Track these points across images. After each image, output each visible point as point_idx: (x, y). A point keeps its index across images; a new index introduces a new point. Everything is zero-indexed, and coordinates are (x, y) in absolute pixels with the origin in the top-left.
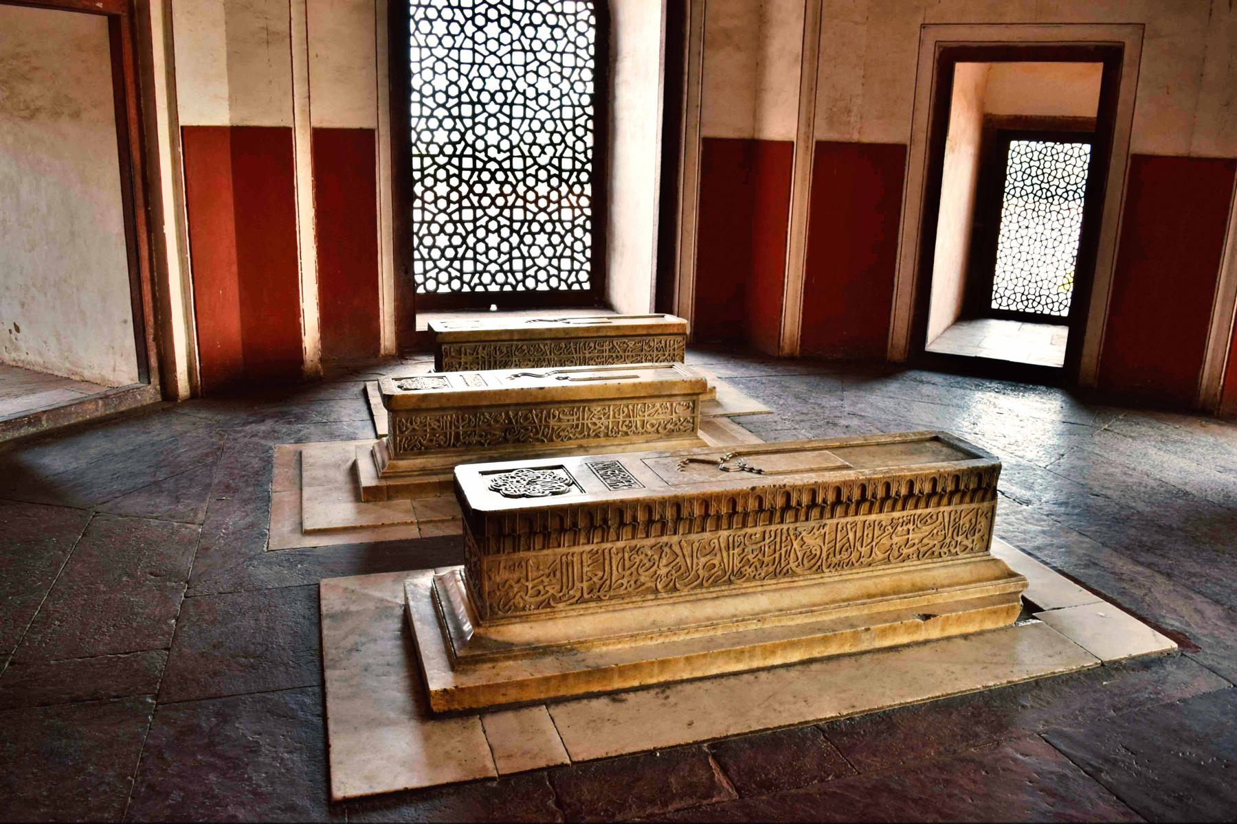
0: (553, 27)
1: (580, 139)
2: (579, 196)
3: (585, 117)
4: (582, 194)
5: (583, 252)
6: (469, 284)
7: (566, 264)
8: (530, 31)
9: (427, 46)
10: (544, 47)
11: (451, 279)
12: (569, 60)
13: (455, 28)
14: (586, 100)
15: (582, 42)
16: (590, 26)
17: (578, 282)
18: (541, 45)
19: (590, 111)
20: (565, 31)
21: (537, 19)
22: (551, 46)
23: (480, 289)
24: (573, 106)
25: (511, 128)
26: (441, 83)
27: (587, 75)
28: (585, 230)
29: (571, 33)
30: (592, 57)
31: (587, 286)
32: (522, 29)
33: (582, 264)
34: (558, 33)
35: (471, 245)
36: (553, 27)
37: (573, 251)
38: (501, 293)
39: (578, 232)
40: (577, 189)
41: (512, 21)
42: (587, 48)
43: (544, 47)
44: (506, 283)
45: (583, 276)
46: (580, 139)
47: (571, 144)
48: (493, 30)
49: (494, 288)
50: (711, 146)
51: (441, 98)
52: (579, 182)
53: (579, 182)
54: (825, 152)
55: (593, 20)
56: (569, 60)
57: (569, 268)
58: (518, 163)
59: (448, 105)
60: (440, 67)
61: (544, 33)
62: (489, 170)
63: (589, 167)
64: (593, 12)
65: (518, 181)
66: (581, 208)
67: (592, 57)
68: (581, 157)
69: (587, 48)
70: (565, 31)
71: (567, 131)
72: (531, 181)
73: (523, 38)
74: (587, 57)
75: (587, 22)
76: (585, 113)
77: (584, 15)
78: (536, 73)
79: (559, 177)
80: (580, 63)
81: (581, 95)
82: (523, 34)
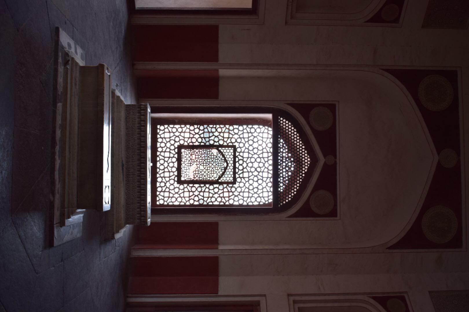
0: (257, 188)
4: (194, 201)
6: (160, 155)
7: (167, 194)
8: (256, 179)
9: (249, 140)
11: (162, 148)
12: (246, 195)
15: (253, 199)
18: (251, 183)
21: (260, 182)
23: (158, 159)
27: (241, 202)
28: (180, 202)
30: (248, 204)
31: (158, 203)
34: (256, 190)
37: (172, 197)
39: (179, 199)
40: (196, 199)
41: (259, 172)
42: (251, 202)
44: (160, 169)
45: (161, 202)
47: (214, 196)
48: (256, 165)
50: (215, 225)
54: (215, 260)
55: (261, 203)
56: (246, 195)
57: (165, 196)
61: (255, 185)
64: (264, 204)
67: (248, 204)
68: (209, 200)
69: (251, 202)
71: (219, 194)
74: (248, 202)
76: (226, 201)
77: (263, 201)
79: (201, 191)
80: (245, 199)
82: (255, 176)
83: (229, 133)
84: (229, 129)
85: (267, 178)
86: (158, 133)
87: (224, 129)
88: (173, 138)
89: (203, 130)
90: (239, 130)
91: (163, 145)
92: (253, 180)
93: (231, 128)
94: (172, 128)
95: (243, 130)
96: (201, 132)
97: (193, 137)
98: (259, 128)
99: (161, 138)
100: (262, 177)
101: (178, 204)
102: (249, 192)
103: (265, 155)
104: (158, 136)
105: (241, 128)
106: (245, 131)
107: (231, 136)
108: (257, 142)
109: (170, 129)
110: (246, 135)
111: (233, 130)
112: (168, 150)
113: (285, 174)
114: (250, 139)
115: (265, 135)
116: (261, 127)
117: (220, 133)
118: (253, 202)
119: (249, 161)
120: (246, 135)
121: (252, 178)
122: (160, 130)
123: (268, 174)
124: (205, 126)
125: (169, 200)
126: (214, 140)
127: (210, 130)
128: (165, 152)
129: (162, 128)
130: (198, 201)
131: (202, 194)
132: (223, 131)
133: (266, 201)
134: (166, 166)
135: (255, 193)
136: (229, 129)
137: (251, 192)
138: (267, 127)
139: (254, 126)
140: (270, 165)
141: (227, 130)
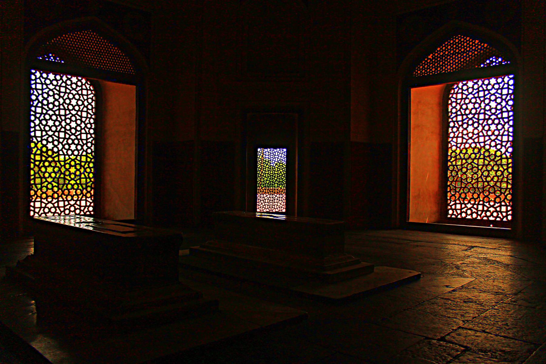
26: (470, 129)
38: (495, 221)
44: (497, 217)
49: (491, 218)
60: (470, 122)
84: (453, 138)
87: (453, 144)
93: (452, 135)
98: (451, 104)
110: (460, 118)
120: (460, 118)
128: (477, 209)
136: (453, 138)
141: (455, 140)
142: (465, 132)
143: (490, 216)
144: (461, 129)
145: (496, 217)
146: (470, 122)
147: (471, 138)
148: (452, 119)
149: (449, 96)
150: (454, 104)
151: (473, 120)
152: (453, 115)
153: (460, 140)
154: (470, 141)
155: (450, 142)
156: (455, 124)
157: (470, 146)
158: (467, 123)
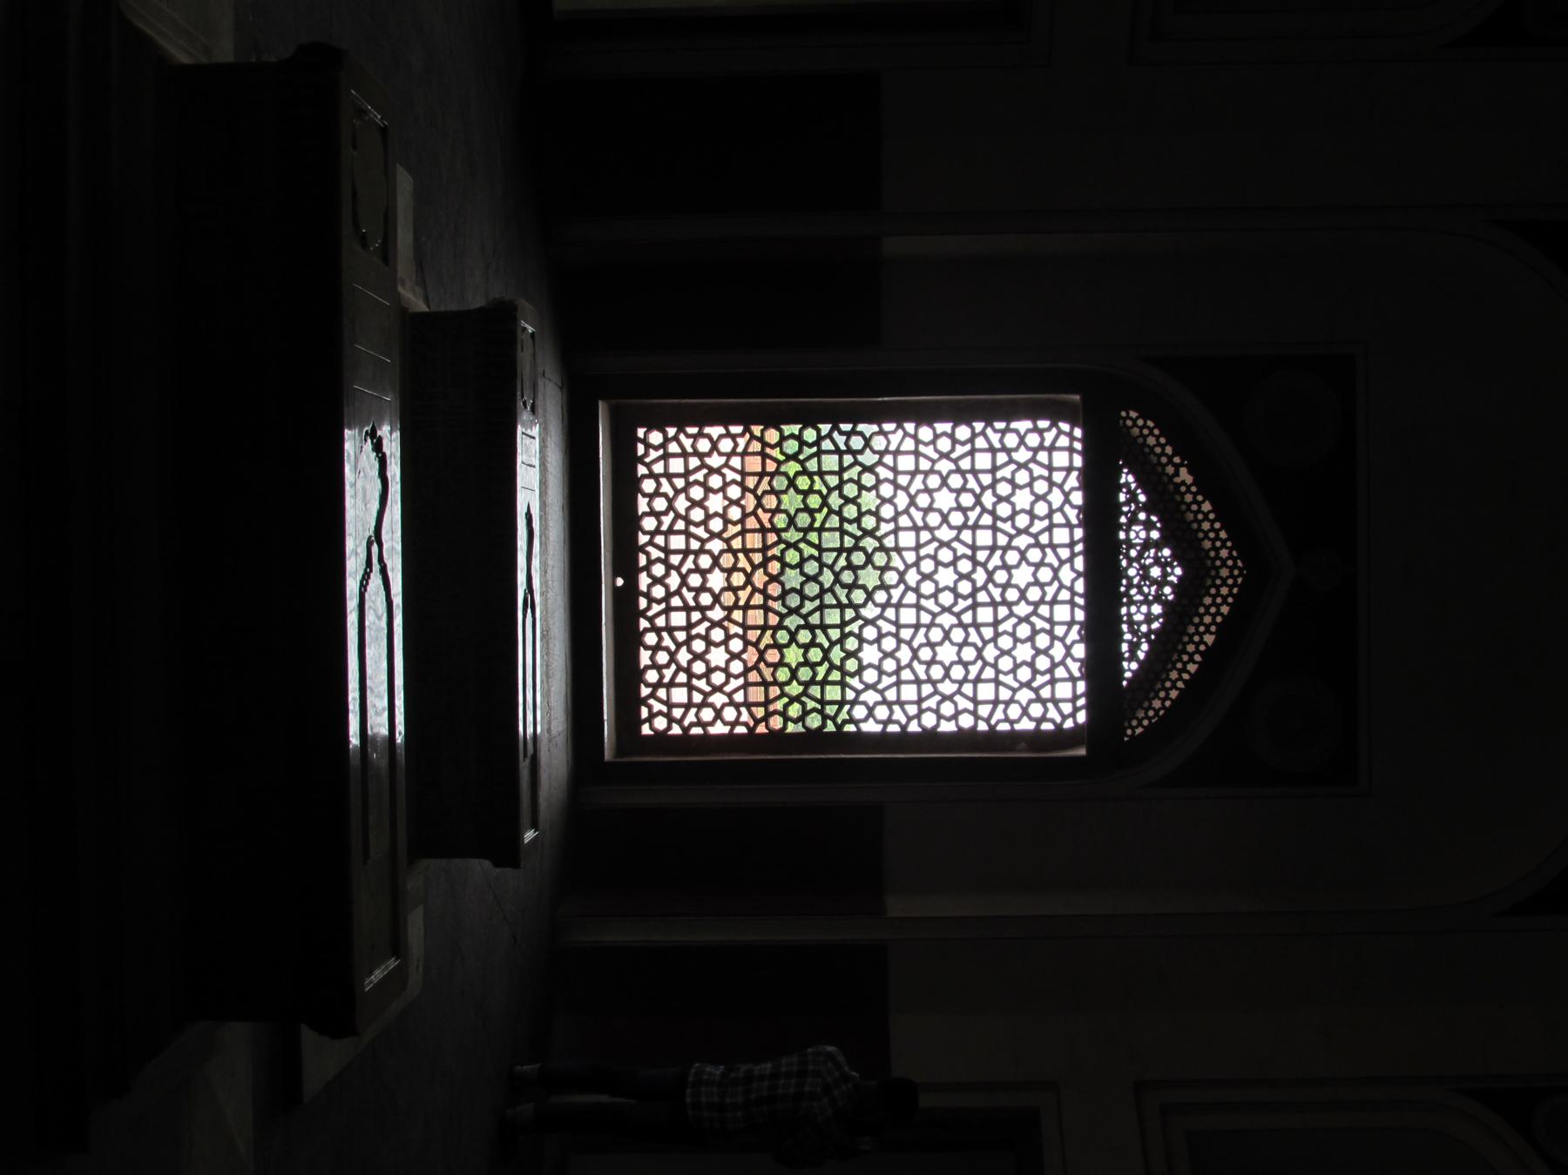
0: (1031, 665)
1: (871, 710)
2: (783, 714)
3: (904, 720)
4: (787, 719)
5: (699, 723)
6: (651, 543)
7: (679, 695)
8: (1024, 631)
10: (1003, 653)
13: (1023, 521)
14: (929, 720)
16: (1039, 721)
17: (652, 716)
19: (914, 727)
20: (1028, 685)
21: (1042, 641)
22: (1006, 664)
23: (643, 560)
24: (920, 701)
25: (884, 606)
26: (945, 500)
27: (966, 721)
29: (1025, 695)
31: (646, 730)
32: (1026, 619)
33: (680, 722)
34: (1024, 674)
35: (708, 546)
36: (1031, 665)
40: (794, 710)
42: (1007, 719)
43: (1003, 653)
44: (651, 600)
45: (660, 723)
46: (871, 710)
49: (644, 581)
51: (923, 501)
52: (805, 713)
53: (805, 713)
56: (986, 691)
58: (833, 617)
59: (912, 510)
60: (967, 500)
62: (821, 572)
63: (830, 727)
65: (805, 617)
66: (766, 719)
68: (843, 715)
69: (1007, 719)
70: (1028, 685)
72: (805, 637)
73: (1014, 620)
75: (1043, 719)
76: (910, 719)
78: (965, 643)
79: (812, 681)
81: (937, 712)
82: (1021, 620)
83: (917, 453)
85: (1070, 624)
86: (641, 460)
87: (895, 439)
88: (699, 476)
89: (817, 443)
90: (955, 441)
91: (660, 505)
92: (1013, 635)
93: (925, 433)
94: (695, 437)
95: (971, 440)
96: (808, 451)
97: (777, 472)
98: (1035, 429)
99: (651, 475)
100: (1050, 620)
101: (726, 730)
102: (997, 683)
103: (1061, 536)
104: (642, 470)
105: (963, 432)
106: (980, 443)
107: (925, 465)
108: (1030, 485)
109: (687, 443)
111: (933, 442)
112: (680, 525)
113: (1142, 614)
114: (999, 475)
115: (1061, 459)
116: (1043, 424)
117: (882, 454)
118: (1012, 722)
119: (996, 561)
120: (983, 461)
121: (1007, 626)
122: (648, 446)
123: (1069, 614)
124: (825, 428)
125: (691, 717)
126: (858, 483)
127: (840, 440)
128: (671, 531)
129: (656, 438)
130: (801, 719)
131: (815, 691)
132: (892, 448)
133: (1064, 717)
134: (673, 588)
135: (1022, 685)
137: (1009, 679)
138: (1065, 427)
139: (1014, 425)
140: (1079, 574)
141: (909, 444)
142: (934, 481)
143: (650, 575)
144: (945, 466)
145: (647, 595)
146: (967, 500)
147: (912, 502)
148: (983, 433)
149: (1065, 421)
150: (1033, 440)
151: (972, 509)
152: (995, 438)
153: (906, 463)
154: (902, 500)
155: (900, 426)
156: (963, 444)
157: (884, 501)
158: (964, 489)
